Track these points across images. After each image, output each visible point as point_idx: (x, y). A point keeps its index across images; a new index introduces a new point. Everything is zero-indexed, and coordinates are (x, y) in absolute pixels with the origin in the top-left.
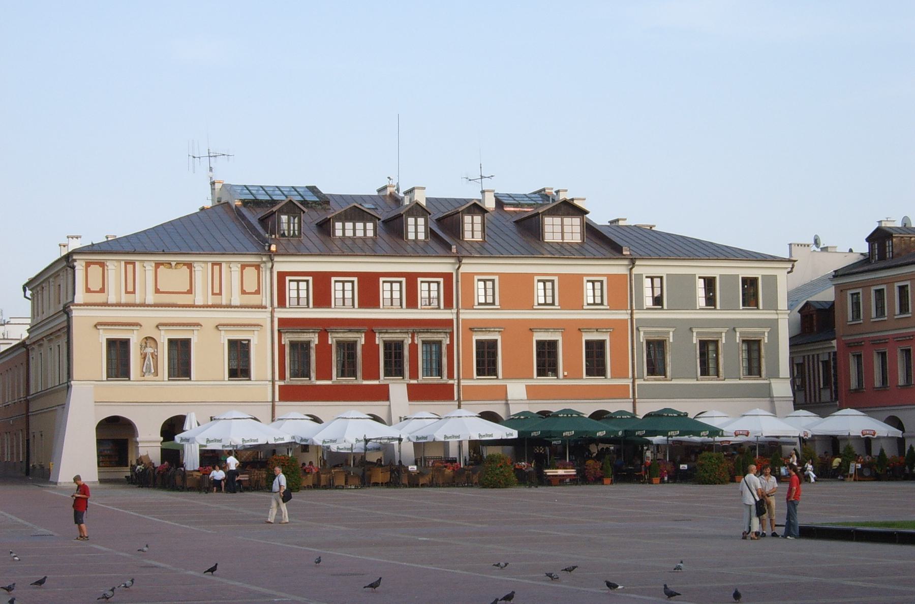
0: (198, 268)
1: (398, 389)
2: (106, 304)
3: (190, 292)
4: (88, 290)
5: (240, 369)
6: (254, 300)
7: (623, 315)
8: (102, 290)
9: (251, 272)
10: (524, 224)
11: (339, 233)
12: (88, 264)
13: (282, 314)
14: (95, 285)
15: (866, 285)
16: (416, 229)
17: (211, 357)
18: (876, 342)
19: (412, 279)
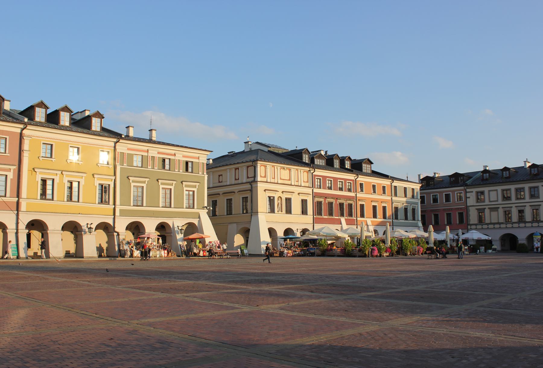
0: (293, 171)
1: (343, 220)
2: (267, 182)
3: (289, 180)
4: (261, 177)
5: (304, 212)
6: (307, 184)
7: (389, 198)
8: (265, 177)
9: (306, 173)
10: (357, 167)
11: (316, 163)
12: (261, 165)
13: (316, 190)
14: (263, 175)
15: (453, 192)
16: (337, 163)
17: (296, 207)
18: (432, 211)
19: (345, 180)
